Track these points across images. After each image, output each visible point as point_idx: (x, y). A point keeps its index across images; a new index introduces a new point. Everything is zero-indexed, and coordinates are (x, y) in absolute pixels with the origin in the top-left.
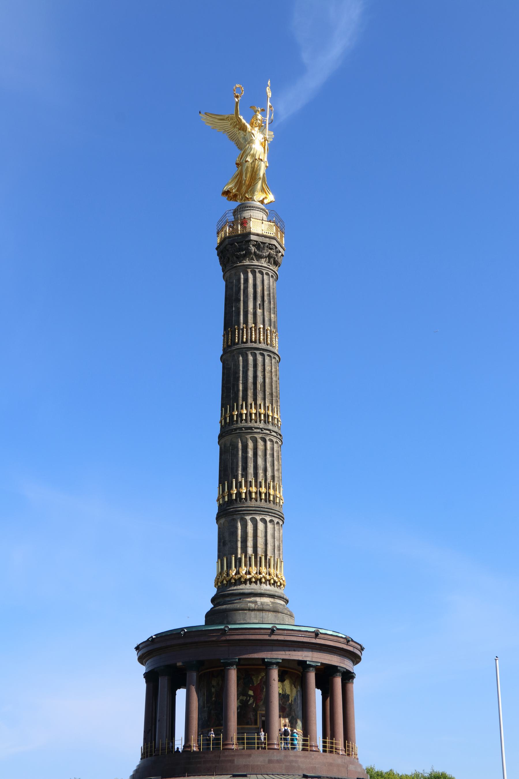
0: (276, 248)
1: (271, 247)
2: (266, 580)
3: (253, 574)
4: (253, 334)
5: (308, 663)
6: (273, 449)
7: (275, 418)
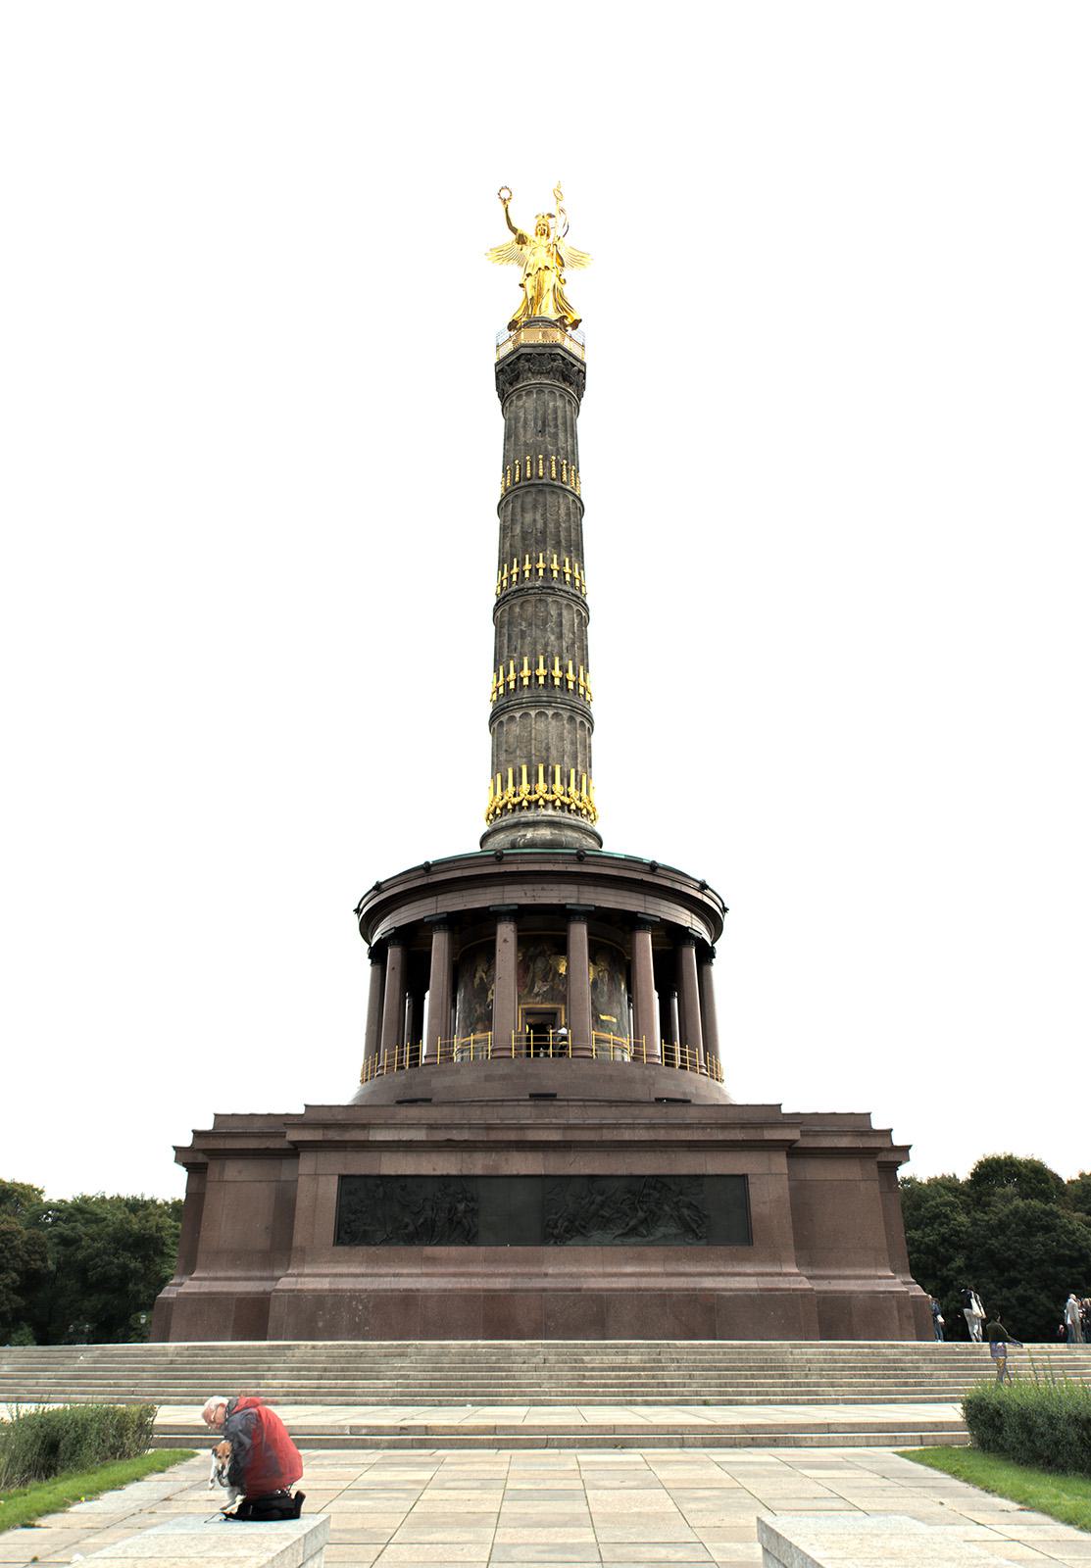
0: (564, 359)
1: (553, 357)
2: (546, 801)
3: (522, 795)
4: (529, 468)
5: (568, 907)
6: (560, 615)
7: (565, 573)
